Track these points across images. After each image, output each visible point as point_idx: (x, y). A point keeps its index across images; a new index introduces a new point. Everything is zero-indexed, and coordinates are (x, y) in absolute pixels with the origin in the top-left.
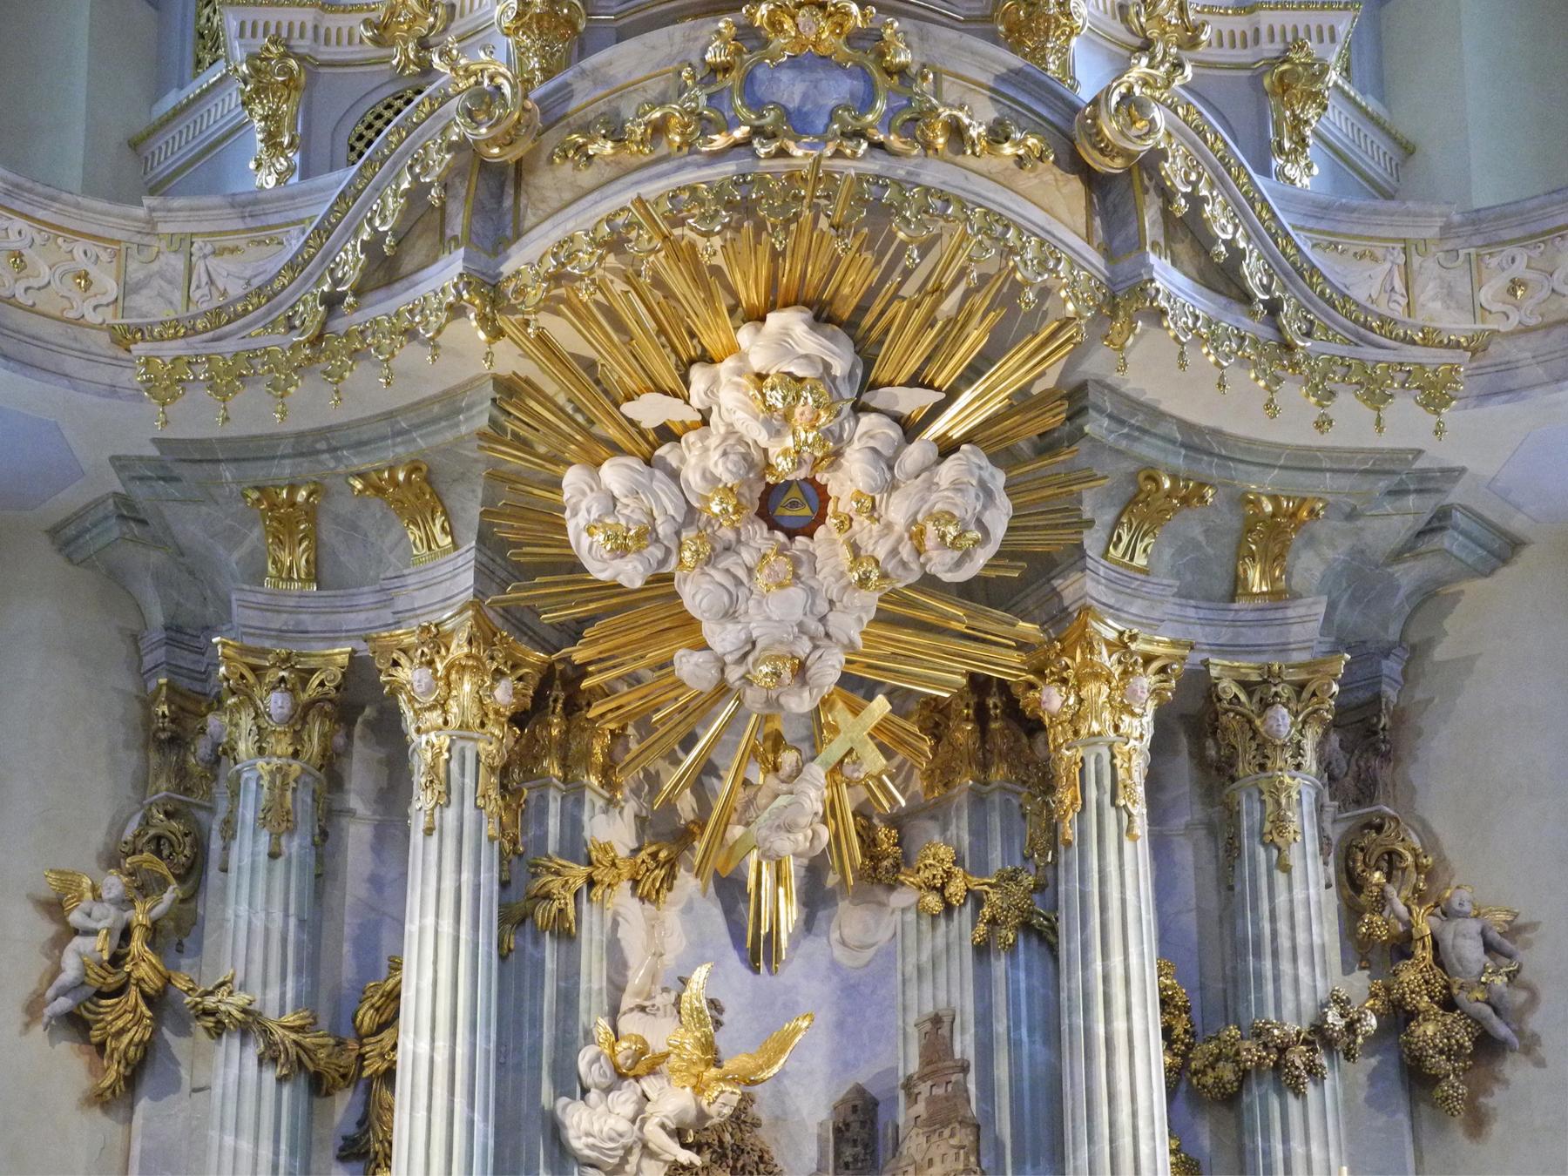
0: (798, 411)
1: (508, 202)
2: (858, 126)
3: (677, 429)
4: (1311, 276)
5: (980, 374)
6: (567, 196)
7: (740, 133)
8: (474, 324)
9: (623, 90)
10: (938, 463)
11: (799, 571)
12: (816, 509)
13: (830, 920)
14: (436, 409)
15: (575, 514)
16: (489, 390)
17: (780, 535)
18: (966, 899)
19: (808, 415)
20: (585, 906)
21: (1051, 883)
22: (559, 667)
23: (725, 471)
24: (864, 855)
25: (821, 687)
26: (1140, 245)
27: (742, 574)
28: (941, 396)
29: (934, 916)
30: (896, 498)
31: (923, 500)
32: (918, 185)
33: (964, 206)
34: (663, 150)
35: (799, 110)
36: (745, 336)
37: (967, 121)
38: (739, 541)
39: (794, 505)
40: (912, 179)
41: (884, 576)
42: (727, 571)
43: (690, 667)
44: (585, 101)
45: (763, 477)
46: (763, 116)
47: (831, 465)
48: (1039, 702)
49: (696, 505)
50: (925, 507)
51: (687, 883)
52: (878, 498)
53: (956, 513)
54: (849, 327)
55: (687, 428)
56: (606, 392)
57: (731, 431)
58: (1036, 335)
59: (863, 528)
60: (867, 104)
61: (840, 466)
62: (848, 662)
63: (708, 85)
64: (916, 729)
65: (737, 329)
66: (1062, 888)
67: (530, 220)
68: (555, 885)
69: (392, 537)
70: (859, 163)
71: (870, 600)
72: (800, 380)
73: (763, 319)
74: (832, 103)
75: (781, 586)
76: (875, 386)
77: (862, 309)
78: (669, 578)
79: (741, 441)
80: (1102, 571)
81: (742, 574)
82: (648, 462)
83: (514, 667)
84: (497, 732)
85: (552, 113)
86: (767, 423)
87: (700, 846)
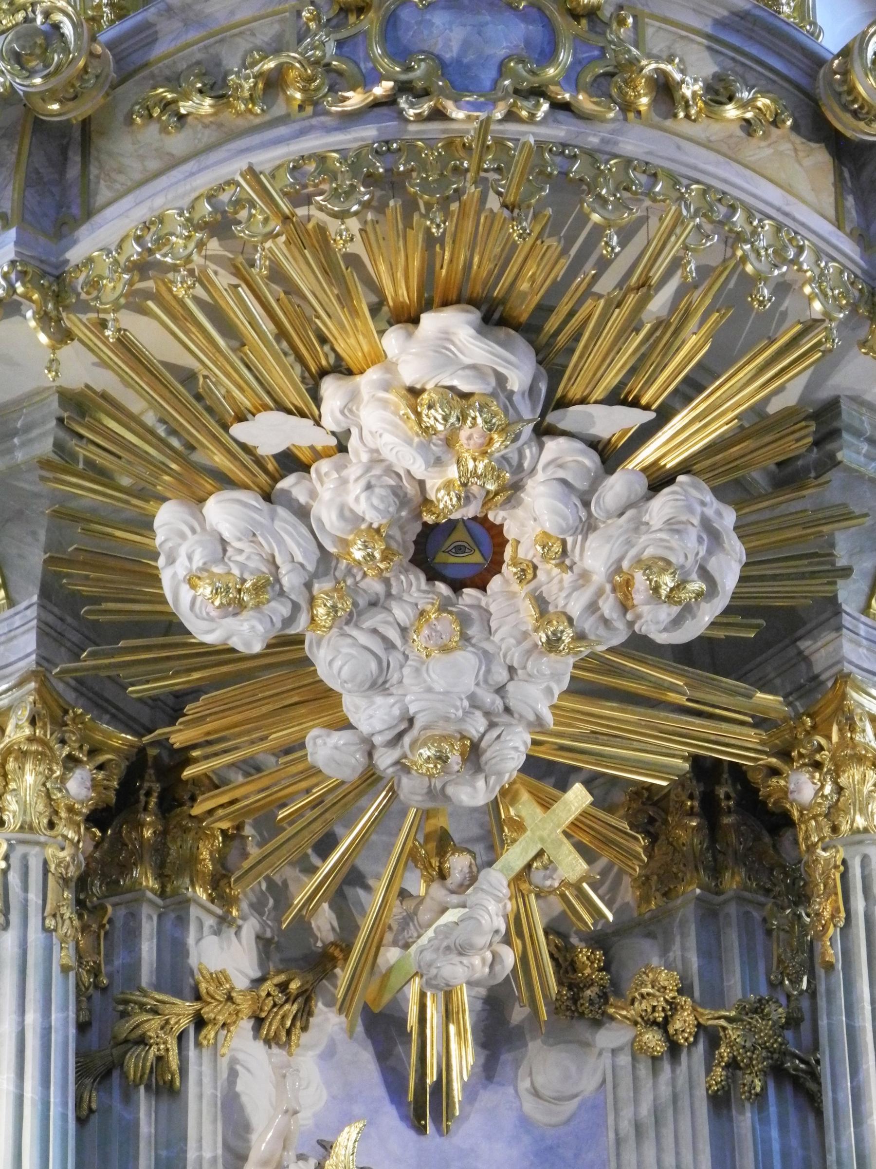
0: (464, 434)
1: (73, 172)
2: (535, 81)
3: (304, 456)
5: (700, 389)
7: (381, 89)
8: (33, 324)
9: (224, 35)
11: (468, 630)
13: (517, 1064)
15: (171, 561)
16: (54, 405)
17: (442, 588)
18: (696, 1037)
19: (477, 439)
20: (192, 1053)
21: (807, 1016)
22: (152, 752)
23: (371, 509)
24: (560, 983)
25: (500, 774)
27: (393, 635)
28: (650, 416)
29: (654, 1058)
31: (629, 544)
32: (615, 156)
33: (677, 182)
35: (458, 61)
36: (393, 341)
37: (678, 77)
38: (389, 595)
39: (460, 549)
40: (608, 148)
41: (580, 637)
42: (375, 631)
43: (326, 749)
44: (172, 47)
45: (419, 516)
46: (410, 69)
47: (508, 500)
48: (785, 791)
49: (332, 549)
50: (632, 553)
51: (328, 1021)
52: (570, 540)
53: (673, 559)
54: (529, 330)
56: (210, 410)
57: (376, 459)
58: (772, 342)
59: (552, 579)
60: (549, 56)
61: (520, 502)
62: (535, 743)
63: (337, 28)
64: (626, 826)
65: (381, 333)
66: (823, 1022)
67: (104, 193)
68: (152, 1026)
70: (538, 127)
71: (560, 669)
72: (466, 396)
73: (415, 321)
74: (502, 53)
75: (445, 649)
76: (563, 403)
78: (298, 640)
79: (390, 470)
80: (862, 630)
81: (393, 635)
82: (267, 497)
83: (93, 752)
84: (71, 834)
86: (423, 448)
87: (343, 975)
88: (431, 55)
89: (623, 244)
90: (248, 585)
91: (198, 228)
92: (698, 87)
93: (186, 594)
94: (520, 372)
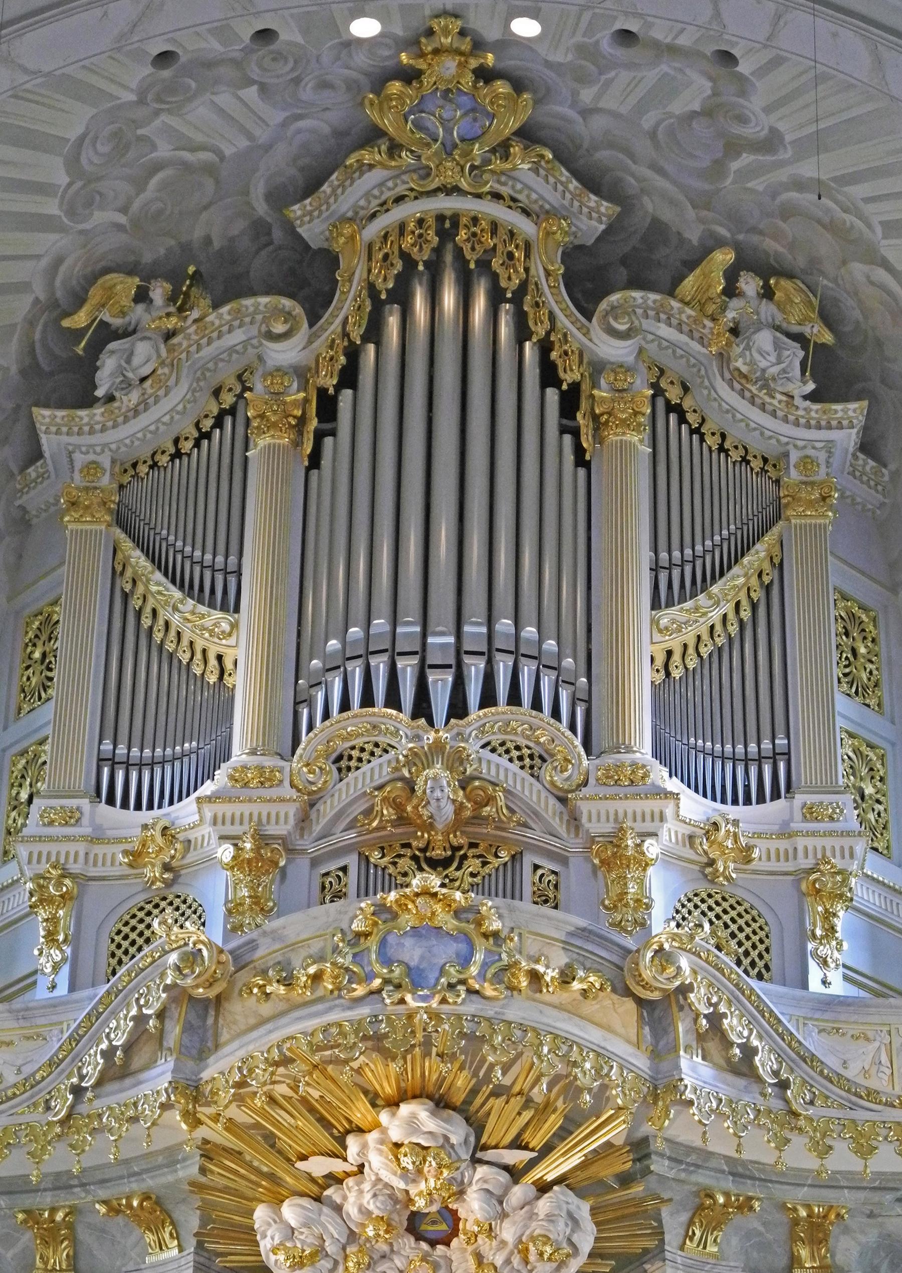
4: (812, 1061)
6: (252, 1021)
10: (538, 1198)
12: (451, 1224)
14: (160, 1159)
15: (264, 1236)
26: (676, 1049)
28: (535, 1154)
30: (506, 1224)
31: (526, 1227)
34: (320, 992)
38: (392, 1251)
40: (499, 1017)
50: (528, 1233)
55: (348, 1175)
57: (379, 1180)
58: (598, 1118)
67: (225, 1036)
69: (133, 1239)
72: (426, 1148)
73: (397, 1105)
76: (485, 1148)
77: (468, 1102)
79: (387, 1185)
85: (241, 960)
88: (400, 962)
89: (504, 1074)
90: (307, 1252)
91: (271, 1065)
92: (555, 974)
93: (273, 1258)
94: (458, 1132)
